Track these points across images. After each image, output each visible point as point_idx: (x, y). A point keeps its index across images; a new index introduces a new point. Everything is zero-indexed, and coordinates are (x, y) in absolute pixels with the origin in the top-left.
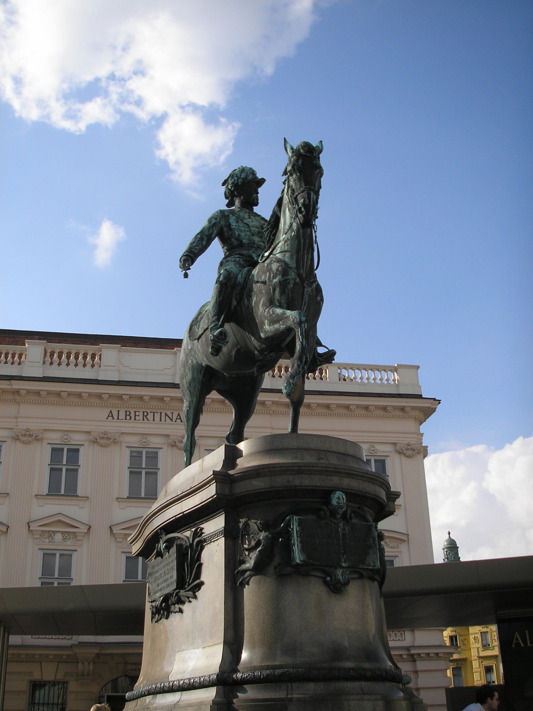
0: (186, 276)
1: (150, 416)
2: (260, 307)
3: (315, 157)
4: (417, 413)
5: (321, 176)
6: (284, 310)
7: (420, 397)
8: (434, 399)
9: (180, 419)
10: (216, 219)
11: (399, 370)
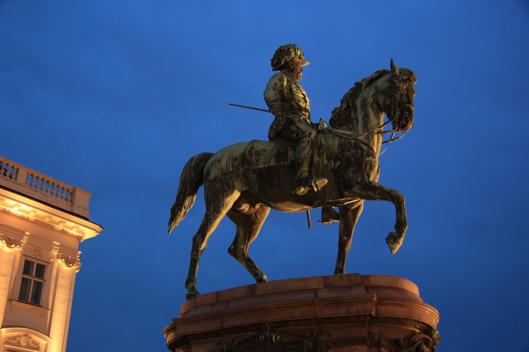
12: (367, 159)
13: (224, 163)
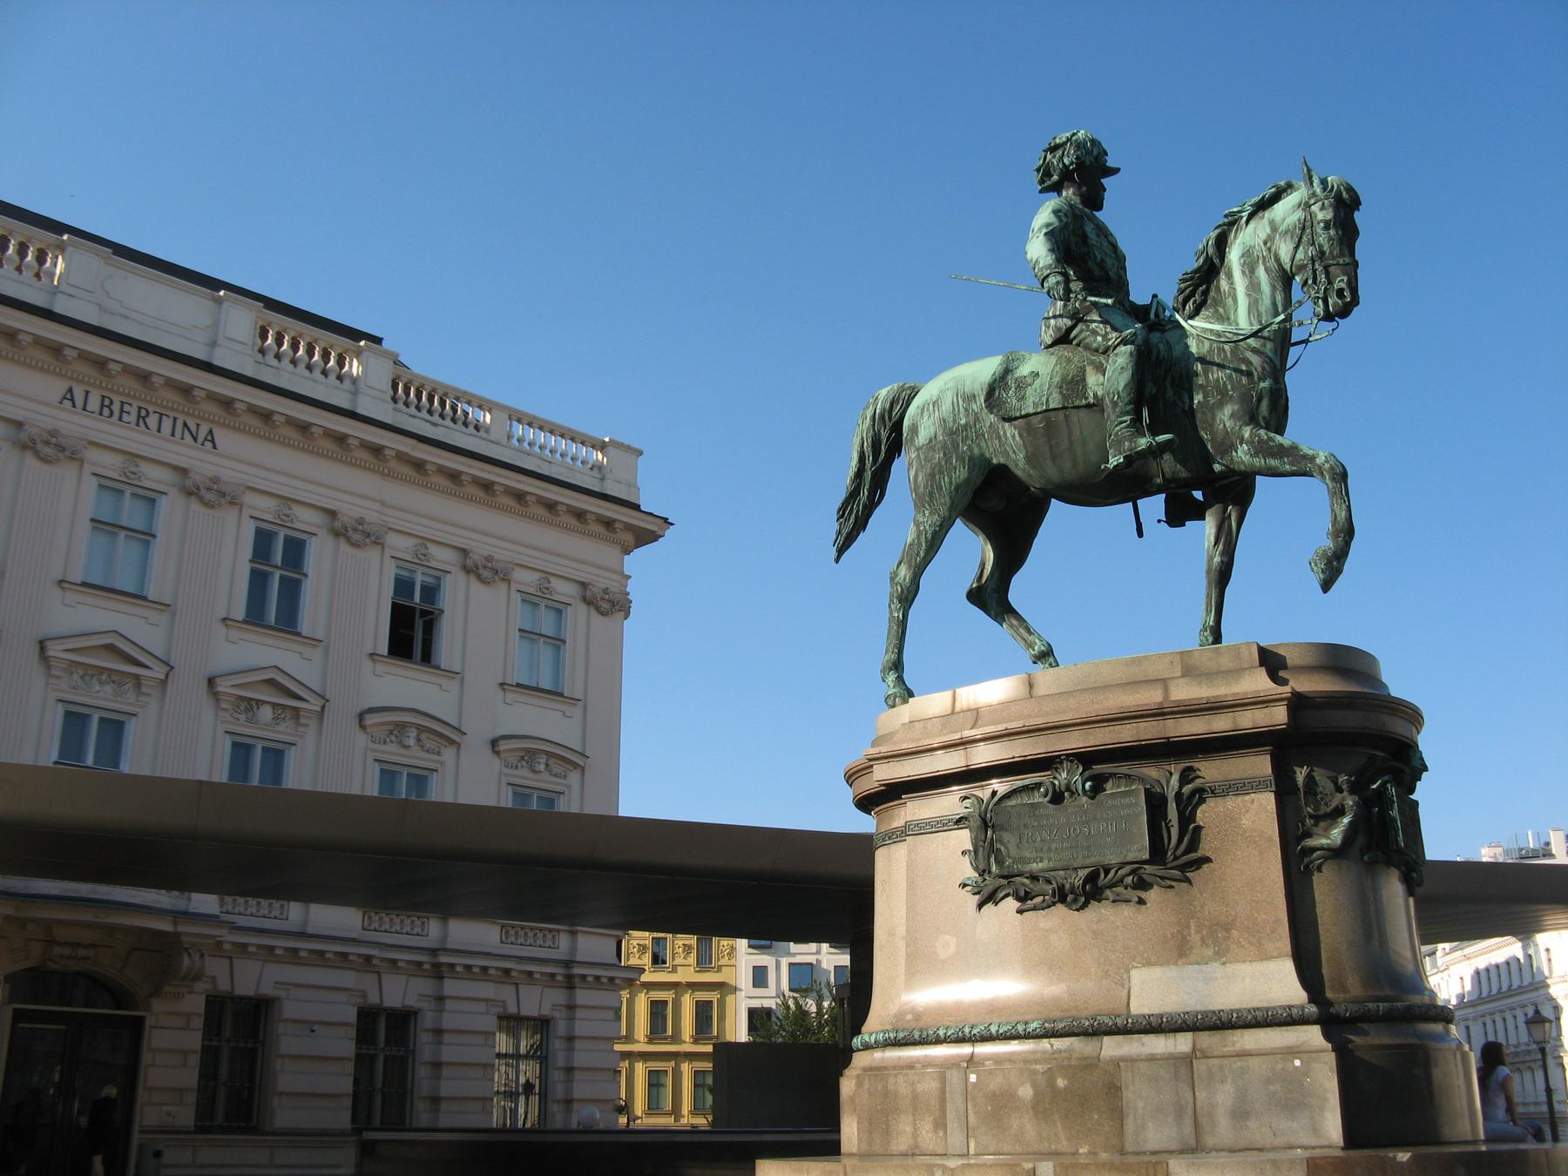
1: (152, 421)
4: (629, 538)
7: (637, 507)
8: (666, 520)
9: (213, 441)
11: (611, 450)
13: (946, 407)
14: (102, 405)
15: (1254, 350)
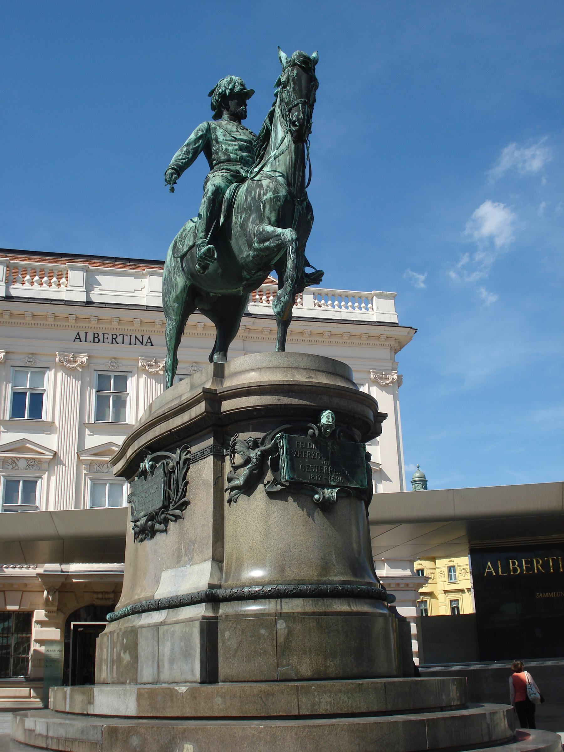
0: (172, 190)
1: (120, 339)
2: (250, 224)
3: (311, 68)
5: (316, 89)
6: (275, 228)
9: (151, 342)
10: (202, 131)
12: (265, 197)
14: (94, 337)
15: (269, 177)
